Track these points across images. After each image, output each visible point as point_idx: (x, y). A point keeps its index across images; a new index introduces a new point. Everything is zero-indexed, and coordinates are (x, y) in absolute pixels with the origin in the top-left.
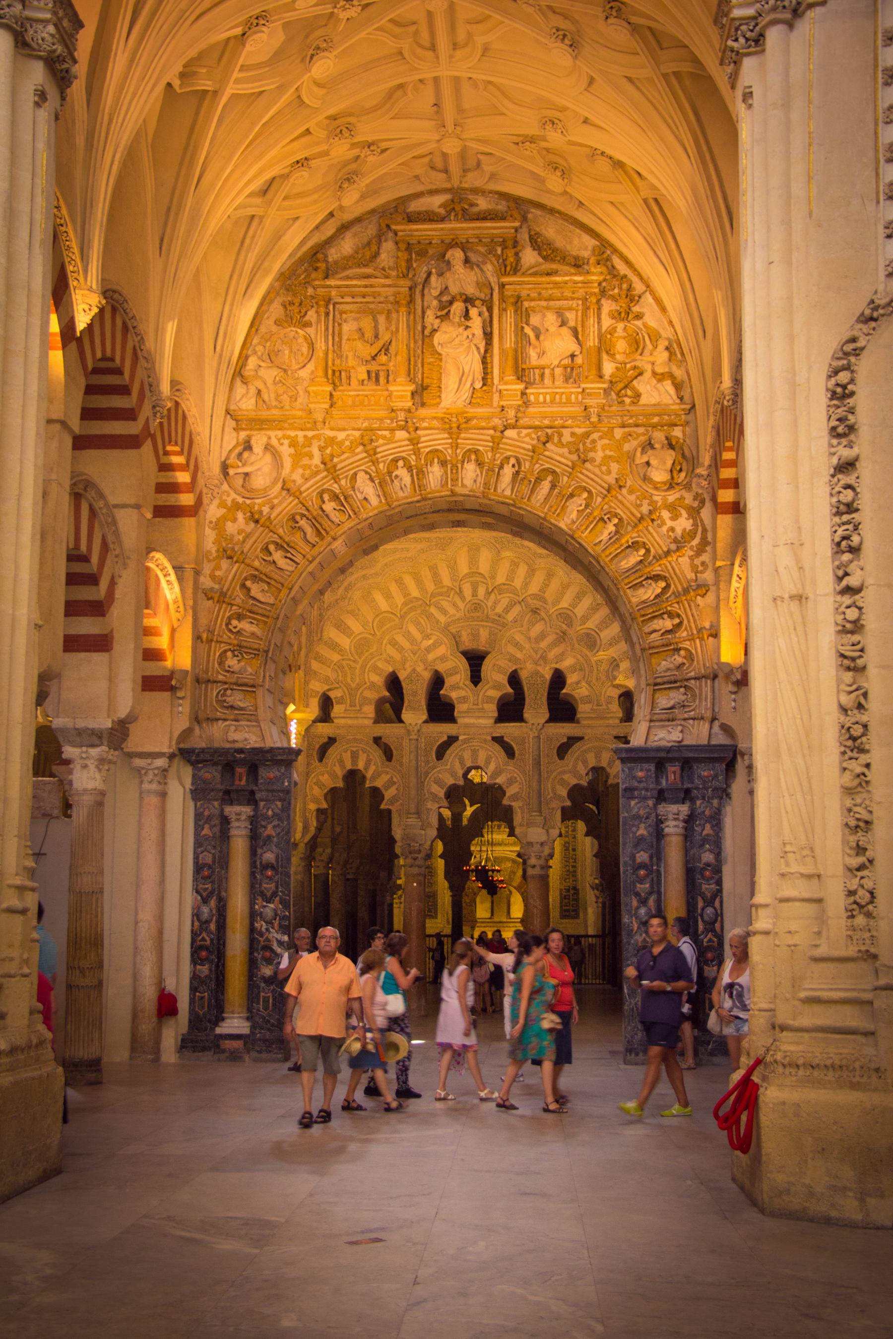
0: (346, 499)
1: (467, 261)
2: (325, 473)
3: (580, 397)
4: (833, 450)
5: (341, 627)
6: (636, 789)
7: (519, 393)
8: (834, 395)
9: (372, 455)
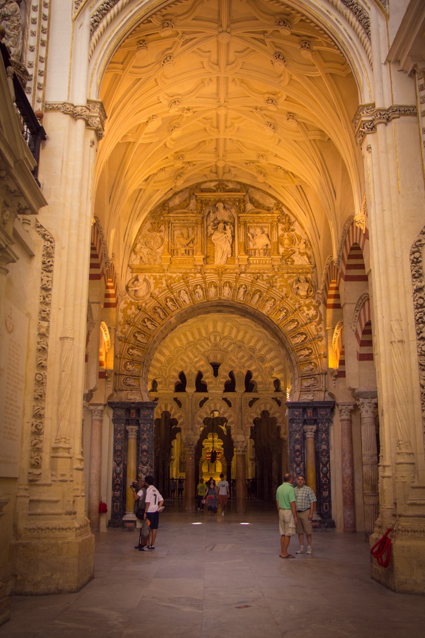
0: (176, 301)
1: (224, 207)
2: (168, 290)
3: (270, 261)
4: (414, 283)
5: (161, 353)
6: (295, 419)
7: (246, 260)
8: (413, 262)
9: (187, 283)
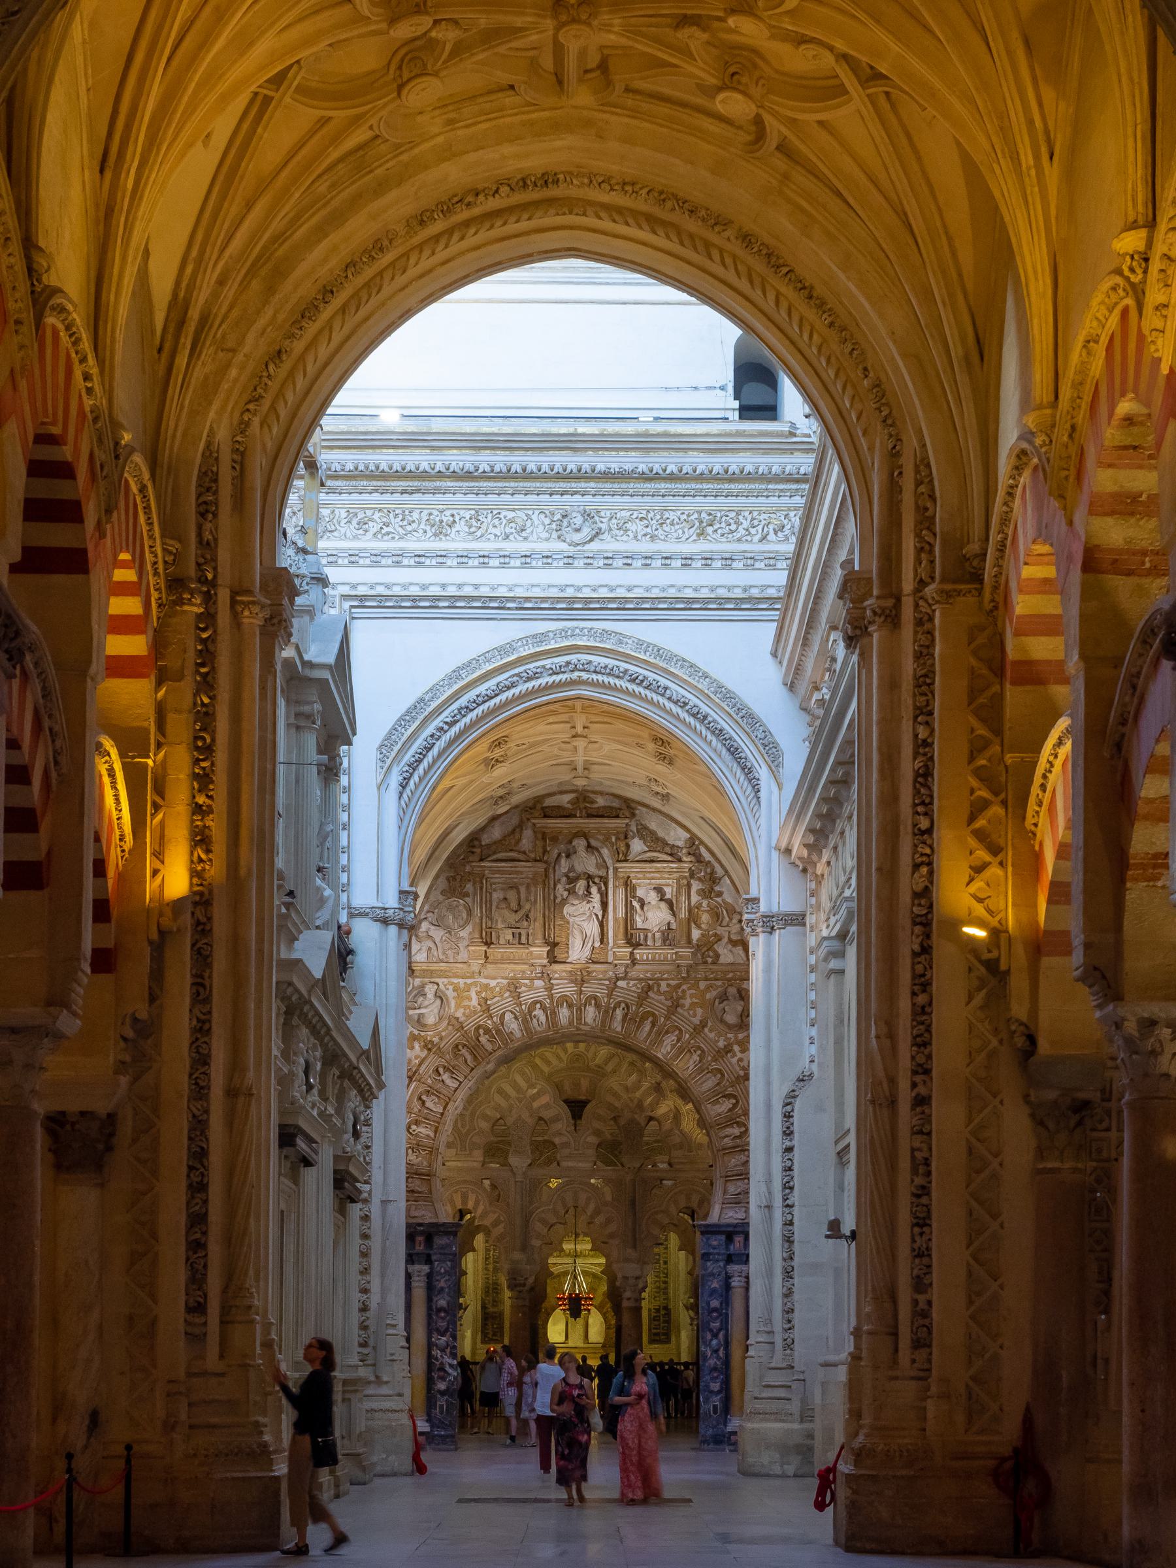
1: (589, 846)
8: (785, 1116)
